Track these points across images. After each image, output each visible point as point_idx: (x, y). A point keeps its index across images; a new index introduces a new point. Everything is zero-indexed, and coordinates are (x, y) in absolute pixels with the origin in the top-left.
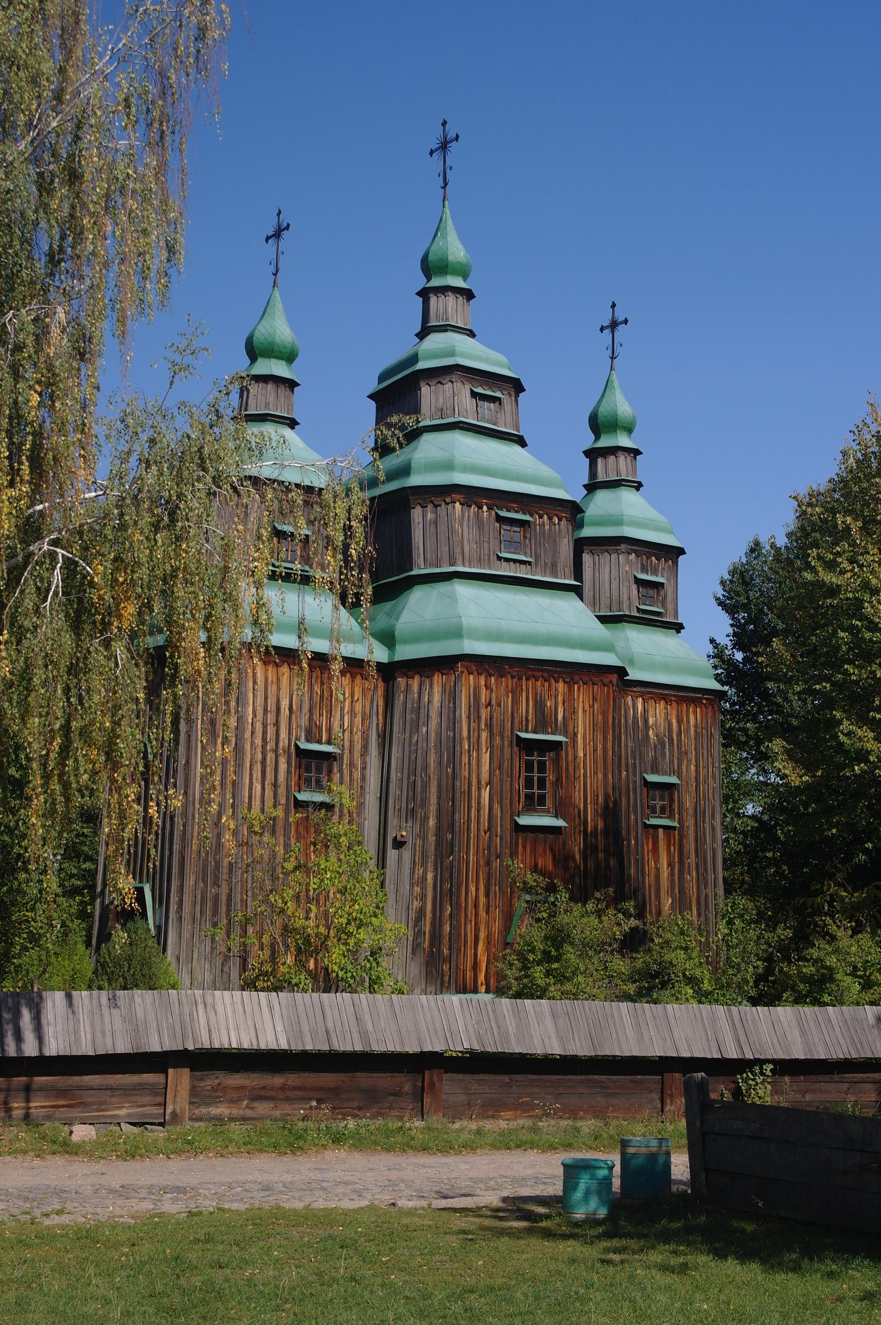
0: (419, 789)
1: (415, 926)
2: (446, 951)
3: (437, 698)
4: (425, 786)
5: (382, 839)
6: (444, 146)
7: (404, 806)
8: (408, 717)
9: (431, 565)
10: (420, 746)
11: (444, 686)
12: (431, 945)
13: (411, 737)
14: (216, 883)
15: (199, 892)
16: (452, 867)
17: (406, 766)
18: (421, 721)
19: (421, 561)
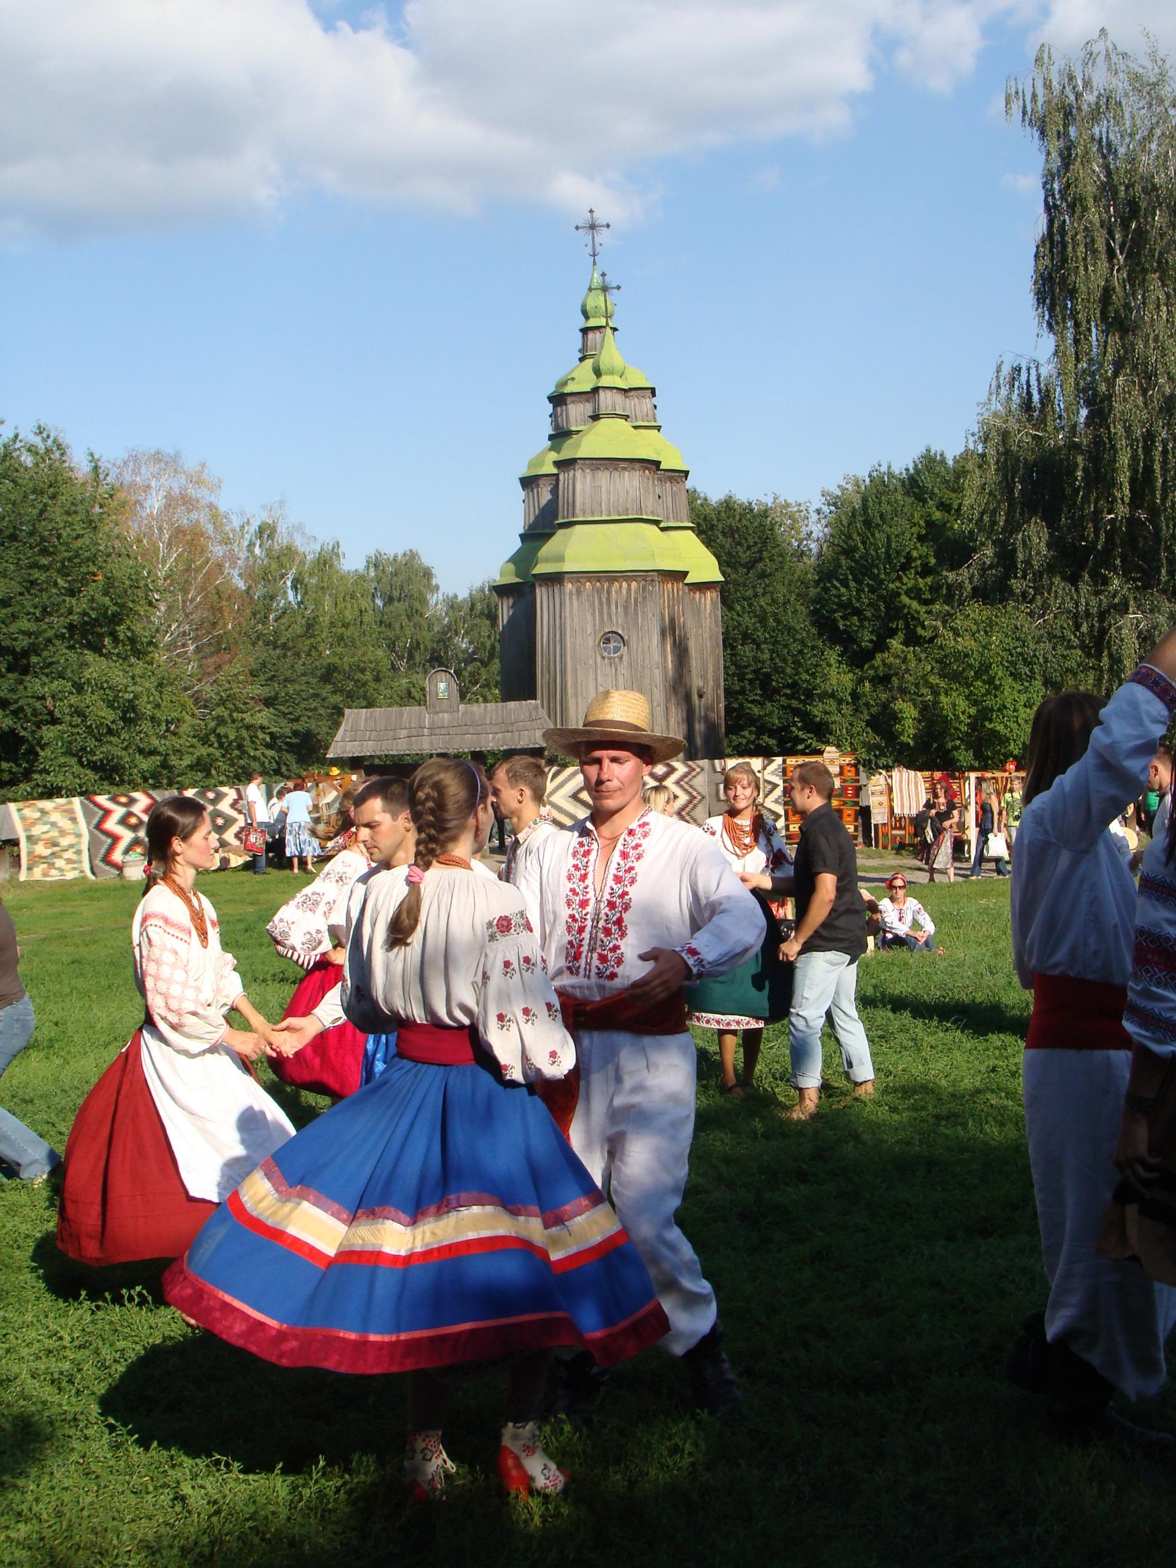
3: (708, 607)
6: (593, 227)
9: (677, 521)
11: (712, 599)
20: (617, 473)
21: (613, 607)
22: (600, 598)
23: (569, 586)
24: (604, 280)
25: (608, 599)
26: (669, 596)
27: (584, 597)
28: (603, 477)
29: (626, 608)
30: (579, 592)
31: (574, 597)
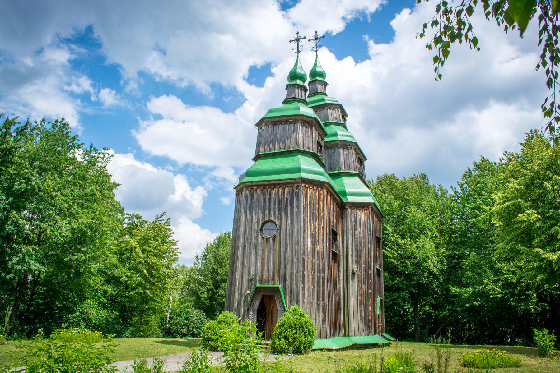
0: (359, 253)
1: (360, 307)
2: (370, 318)
4: (360, 251)
5: (345, 272)
7: (354, 259)
8: (353, 224)
9: (347, 170)
10: (358, 236)
11: (365, 214)
12: (365, 315)
13: (355, 232)
14: (318, 286)
15: (311, 290)
16: (371, 285)
17: (354, 243)
18: (358, 226)
19: (343, 168)
20: (287, 126)
21: (272, 206)
22: (264, 199)
23: (246, 192)
24: (298, 36)
25: (269, 199)
26: (311, 197)
27: (254, 199)
28: (280, 128)
29: (280, 204)
30: (252, 196)
31: (249, 198)
